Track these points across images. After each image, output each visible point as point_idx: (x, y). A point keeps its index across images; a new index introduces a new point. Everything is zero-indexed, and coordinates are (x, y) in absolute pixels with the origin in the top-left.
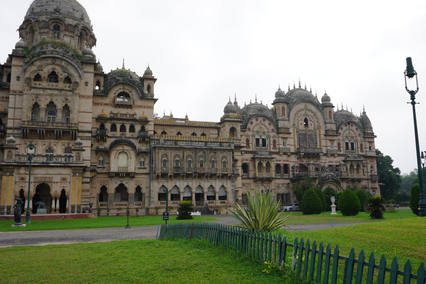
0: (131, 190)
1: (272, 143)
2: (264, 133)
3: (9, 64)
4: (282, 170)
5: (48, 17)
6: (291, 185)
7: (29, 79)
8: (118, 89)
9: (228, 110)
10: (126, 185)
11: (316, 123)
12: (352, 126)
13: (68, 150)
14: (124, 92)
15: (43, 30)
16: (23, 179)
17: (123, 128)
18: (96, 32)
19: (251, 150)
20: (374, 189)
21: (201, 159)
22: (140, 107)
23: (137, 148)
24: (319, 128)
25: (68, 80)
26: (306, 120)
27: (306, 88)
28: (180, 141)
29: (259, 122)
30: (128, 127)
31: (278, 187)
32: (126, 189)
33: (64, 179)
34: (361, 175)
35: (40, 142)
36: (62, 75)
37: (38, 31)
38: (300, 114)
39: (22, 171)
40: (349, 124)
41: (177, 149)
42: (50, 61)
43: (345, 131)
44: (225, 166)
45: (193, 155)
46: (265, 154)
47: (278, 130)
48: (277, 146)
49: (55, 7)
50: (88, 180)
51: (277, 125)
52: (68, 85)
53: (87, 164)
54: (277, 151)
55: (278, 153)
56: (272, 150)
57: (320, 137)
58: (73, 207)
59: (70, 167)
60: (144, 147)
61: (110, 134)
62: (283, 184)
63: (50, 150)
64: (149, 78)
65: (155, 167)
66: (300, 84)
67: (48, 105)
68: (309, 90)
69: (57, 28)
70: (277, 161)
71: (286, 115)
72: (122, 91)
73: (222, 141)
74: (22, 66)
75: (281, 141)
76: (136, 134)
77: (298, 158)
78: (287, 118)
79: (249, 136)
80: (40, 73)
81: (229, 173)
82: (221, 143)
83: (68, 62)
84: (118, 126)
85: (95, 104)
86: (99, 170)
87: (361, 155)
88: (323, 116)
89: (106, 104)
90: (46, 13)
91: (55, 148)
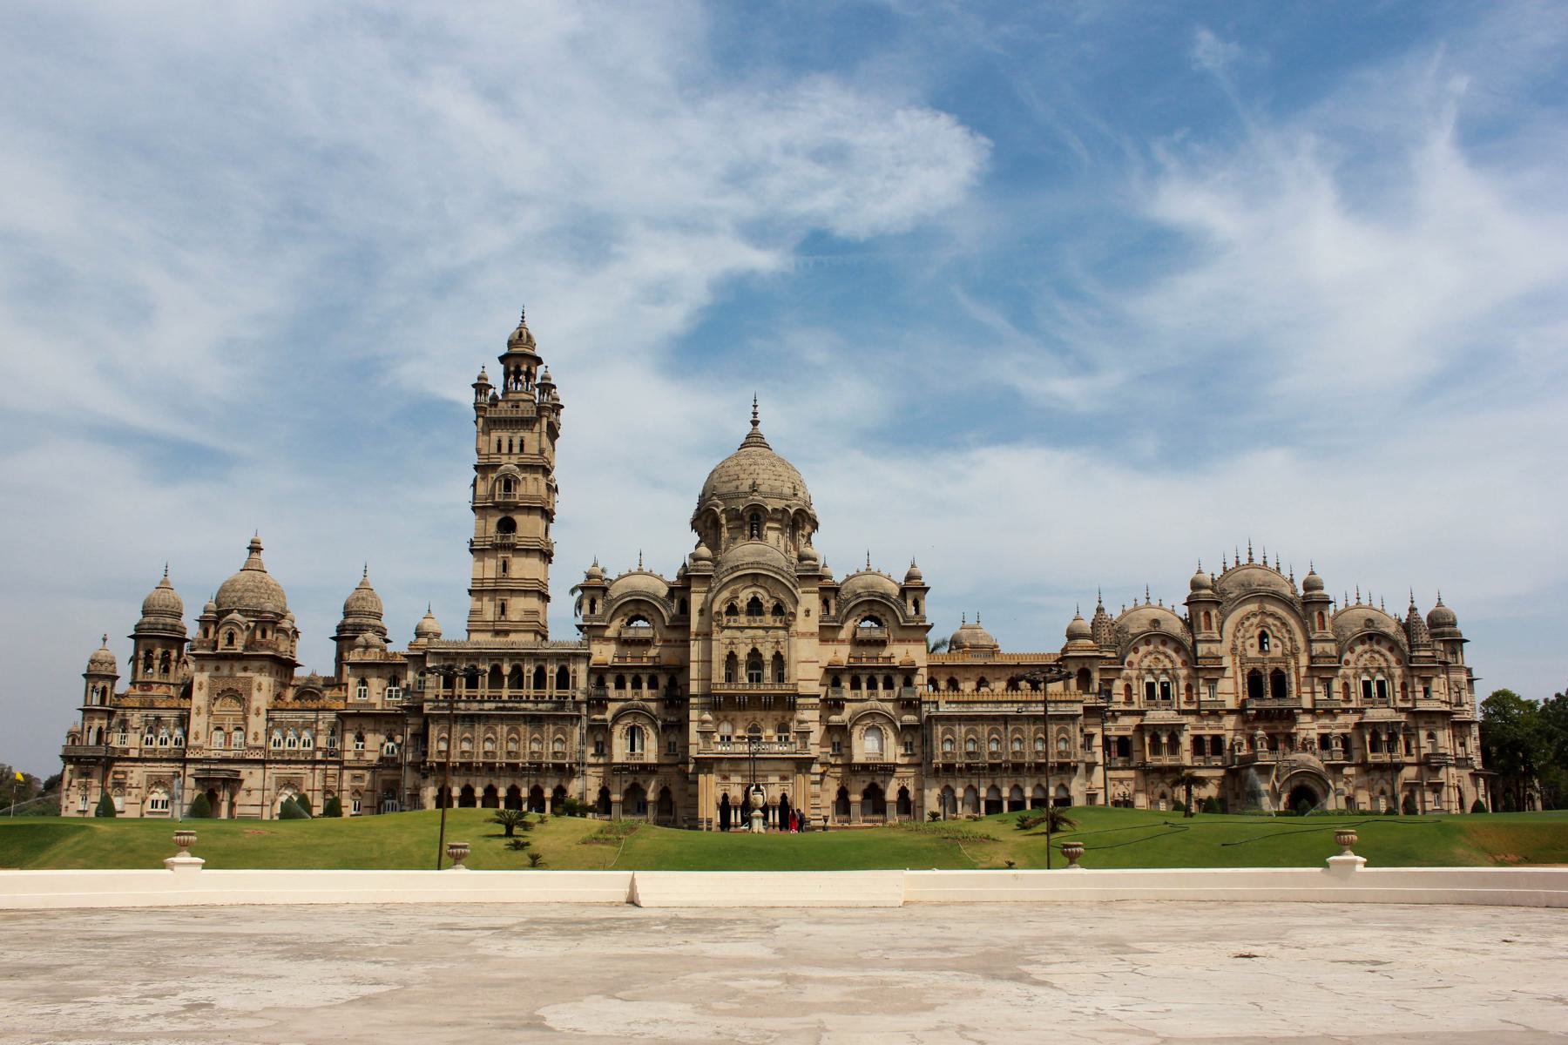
0: (891, 794)
1: (1183, 691)
4: (1208, 747)
7: (719, 613)
9: (1072, 635)
13: (783, 728)
18: (817, 510)
19: (1135, 707)
22: (901, 641)
25: (778, 610)
26: (1263, 636)
34: (1400, 754)
35: (738, 714)
36: (768, 604)
38: (1247, 624)
50: (818, 778)
54: (1193, 707)
55: (1196, 713)
56: (1183, 707)
57: (1297, 673)
60: (910, 718)
63: (755, 729)
68: (1274, 567)
71: (1215, 629)
78: (1217, 636)
79: (1130, 679)
87: (1402, 710)
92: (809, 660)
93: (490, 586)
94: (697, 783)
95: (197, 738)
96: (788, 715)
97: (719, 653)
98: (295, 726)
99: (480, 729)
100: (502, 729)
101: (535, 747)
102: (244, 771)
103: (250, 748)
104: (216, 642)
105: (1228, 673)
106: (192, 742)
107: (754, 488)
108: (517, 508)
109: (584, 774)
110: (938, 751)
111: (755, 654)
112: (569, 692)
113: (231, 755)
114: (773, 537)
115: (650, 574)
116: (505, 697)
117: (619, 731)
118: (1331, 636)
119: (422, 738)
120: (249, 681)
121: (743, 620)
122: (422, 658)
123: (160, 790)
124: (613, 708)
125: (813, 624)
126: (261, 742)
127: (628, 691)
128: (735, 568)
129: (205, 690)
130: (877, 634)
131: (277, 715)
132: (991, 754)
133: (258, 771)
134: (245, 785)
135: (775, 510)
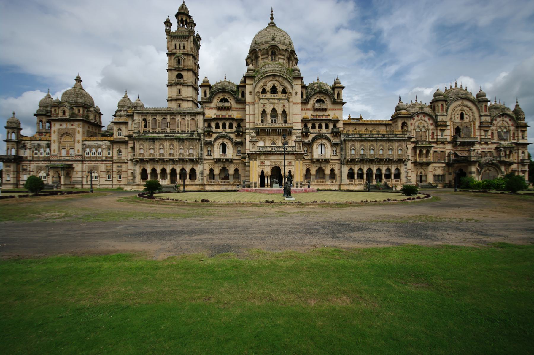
0: (328, 172)
1: (430, 134)
2: (424, 127)
3: (242, 84)
5: (268, 45)
6: (446, 169)
7: (258, 92)
8: (316, 97)
9: (398, 109)
11: (471, 117)
14: (320, 99)
15: (264, 57)
16: (263, 163)
17: (320, 127)
20: (524, 172)
22: (332, 109)
24: (474, 121)
25: (284, 92)
27: (461, 87)
28: (364, 134)
29: (419, 118)
31: (435, 169)
35: (267, 137)
36: (280, 89)
37: (261, 57)
38: (456, 109)
39: (263, 157)
43: (498, 122)
46: (425, 143)
47: (436, 124)
48: (435, 137)
49: (271, 37)
51: (436, 119)
52: (284, 95)
54: (435, 140)
55: (436, 143)
56: (431, 140)
57: (474, 128)
58: (297, 183)
59: (294, 154)
60: (336, 140)
61: (311, 130)
62: (439, 167)
63: (274, 143)
64: (337, 87)
65: (346, 154)
66: (456, 84)
67: (271, 111)
68: (465, 89)
69: (273, 54)
70: (434, 149)
71: (444, 111)
72: (318, 98)
73: (397, 133)
74: (252, 84)
75: (439, 133)
76: (330, 131)
77: (453, 146)
78: (445, 114)
81: (404, 158)
83: (284, 78)
84: (317, 125)
85: (302, 109)
87: (513, 143)
89: (308, 109)
90: (266, 43)
91: (277, 141)
92: (297, 114)
95: (54, 152)
97: (259, 111)
98: (95, 147)
99: (157, 144)
100: (167, 144)
102: (75, 164)
103: (76, 156)
104: (58, 114)
105: (449, 128)
107: (273, 39)
108: (184, 70)
109: (203, 163)
110: (348, 154)
111: (274, 110)
113: (70, 158)
114: (282, 60)
115: (229, 82)
116: (168, 131)
117: (216, 145)
119: (133, 148)
120: (74, 130)
121: (268, 95)
122: (133, 115)
123: (42, 172)
125: (298, 99)
126: (80, 153)
127: (221, 130)
128: (266, 72)
129: (56, 133)
131: (87, 143)
132: (371, 155)
134: (76, 169)
135: (282, 49)
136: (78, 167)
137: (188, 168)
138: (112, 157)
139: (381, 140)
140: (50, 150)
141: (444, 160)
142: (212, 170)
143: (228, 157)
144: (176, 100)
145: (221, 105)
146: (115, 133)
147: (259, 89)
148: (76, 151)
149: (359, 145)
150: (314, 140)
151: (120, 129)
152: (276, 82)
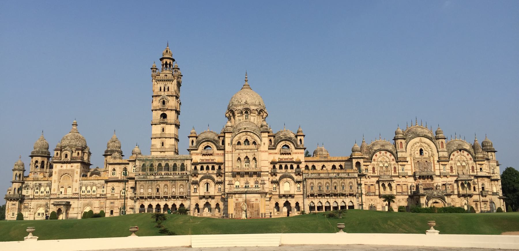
1: (393, 169)
5: (242, 107)
10: (290, 202)
11: (430, 152)
12: (463, 152)
13: (257, 182)
17: (286, 167)
19: (376, 175)
21: (335, 185)
22: (296, 153)
23: (295, 179)
24: (433, 155)
25: (254, 143)
26: (421, 151)
30: (289, 166)
32: (290, 204)
33: (257, 200)
34: (472, 191)
36: (251, 141)
39: (237, 195)
40: (460, 151)
41: (319, 179)
42: (244, 133)
44: (351, 188)
45: (330, 182)
48: (397, 171)
53: (267, 190)
54: (397, 174)
55: (398, 176)
56: (393, 174)
57: (434, 163)
60: (299, 178)
61: (278, 171)
63: (247, 183)
69: (246, 112)
70: (397, 182)
75: (400, 168)
78: (405, 150)
80: (240, 140)
82: (348, 173)
84: (283, 166)
86: (273, 193)
87: (472, 175)
88: (436, 146)
93: (159, 136)
94: (227, 201)
95: (54, 191)
96: (258, 179)
101: (174, 190)
103: (73, 194)
104: (61, 157)
105: (409, 163)
106: (52, 192)
109: (190, 199)
112: (185, 172)
113: (67, 196)
116: (163, 174)
117: (201, 184)
118: (446, 150)
119: (134, 188)
120: (73, 171)
121: (243, 146)
124: (200, 176)
126: (77, 192)
127: (205, 171)
128: (241, 129)
129: (57, 174)
130: (288, 151)
133: (76, 201)
136: (74, 204)
137: (178, 203)
138: (105, 195)
139: (335, 178)
140: (50, 189)
141: (408, 192)
142: (197, 205)
143: (211, 194)
144: (160, 138)
145: (205, 152)
146: (110, 172)
147: (235, 142)
148: (74, 190)
149: (317, 183)
150: (281, 178)
151: (114, 170)
152: (248, 137)
